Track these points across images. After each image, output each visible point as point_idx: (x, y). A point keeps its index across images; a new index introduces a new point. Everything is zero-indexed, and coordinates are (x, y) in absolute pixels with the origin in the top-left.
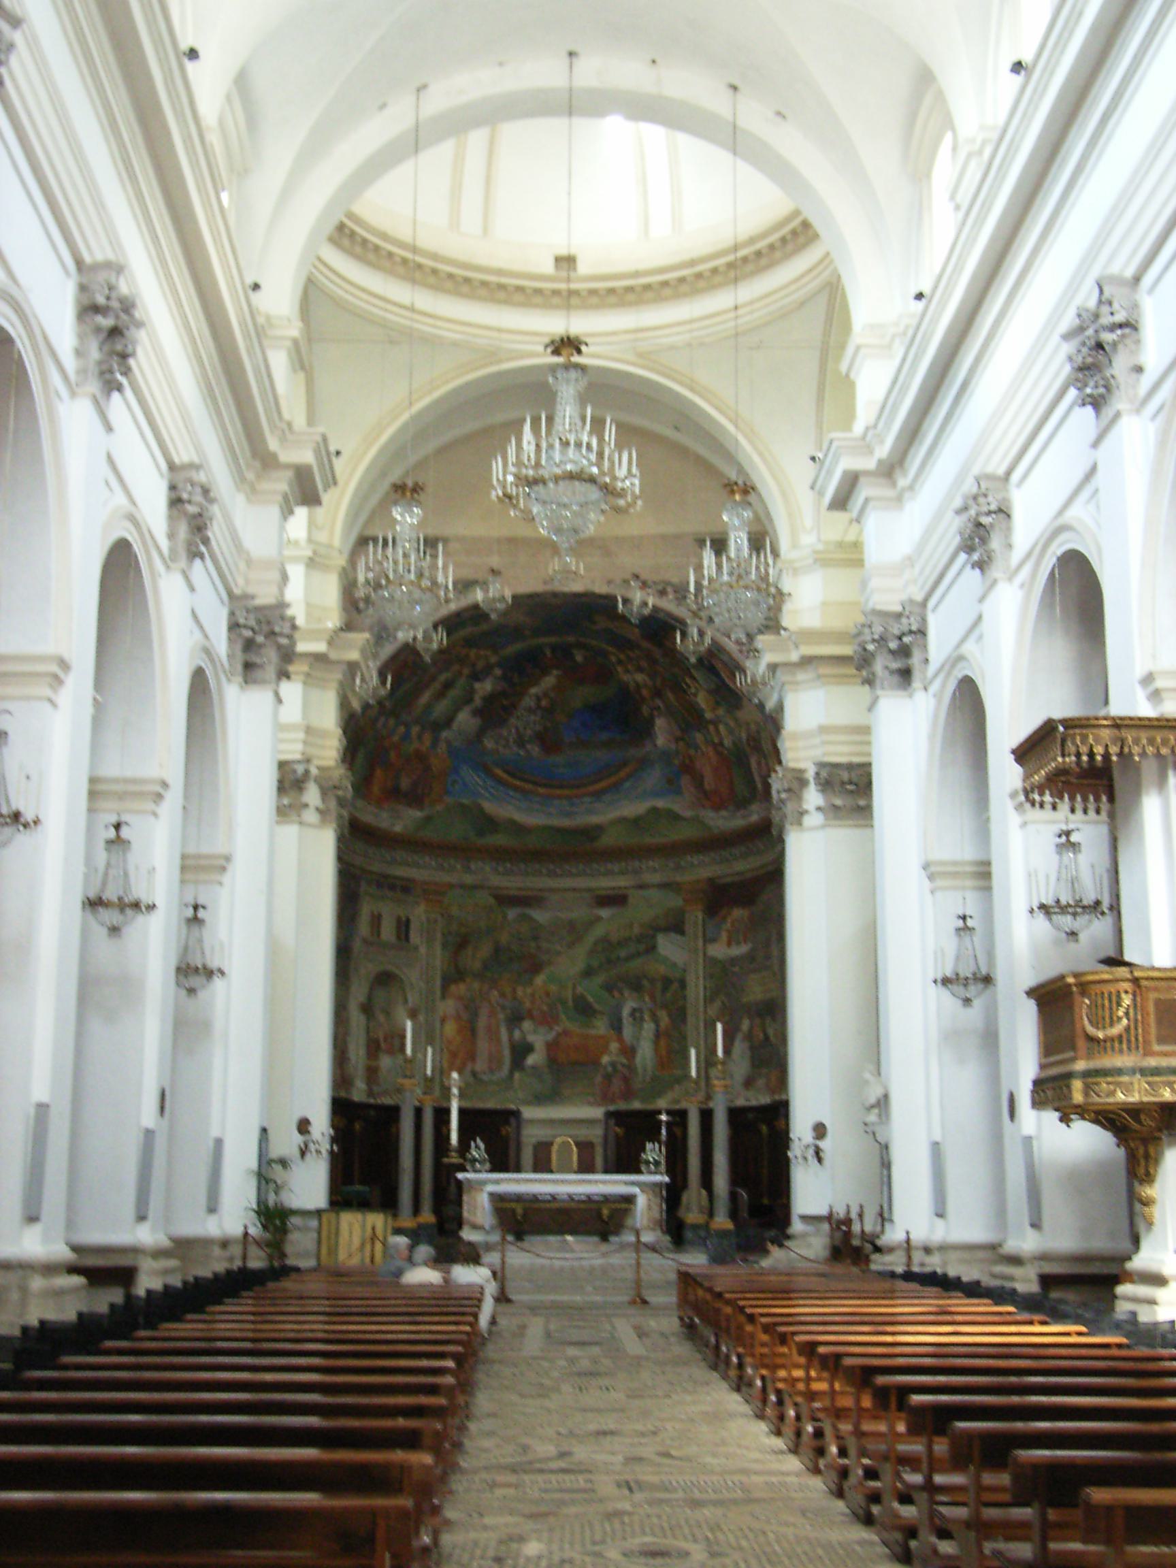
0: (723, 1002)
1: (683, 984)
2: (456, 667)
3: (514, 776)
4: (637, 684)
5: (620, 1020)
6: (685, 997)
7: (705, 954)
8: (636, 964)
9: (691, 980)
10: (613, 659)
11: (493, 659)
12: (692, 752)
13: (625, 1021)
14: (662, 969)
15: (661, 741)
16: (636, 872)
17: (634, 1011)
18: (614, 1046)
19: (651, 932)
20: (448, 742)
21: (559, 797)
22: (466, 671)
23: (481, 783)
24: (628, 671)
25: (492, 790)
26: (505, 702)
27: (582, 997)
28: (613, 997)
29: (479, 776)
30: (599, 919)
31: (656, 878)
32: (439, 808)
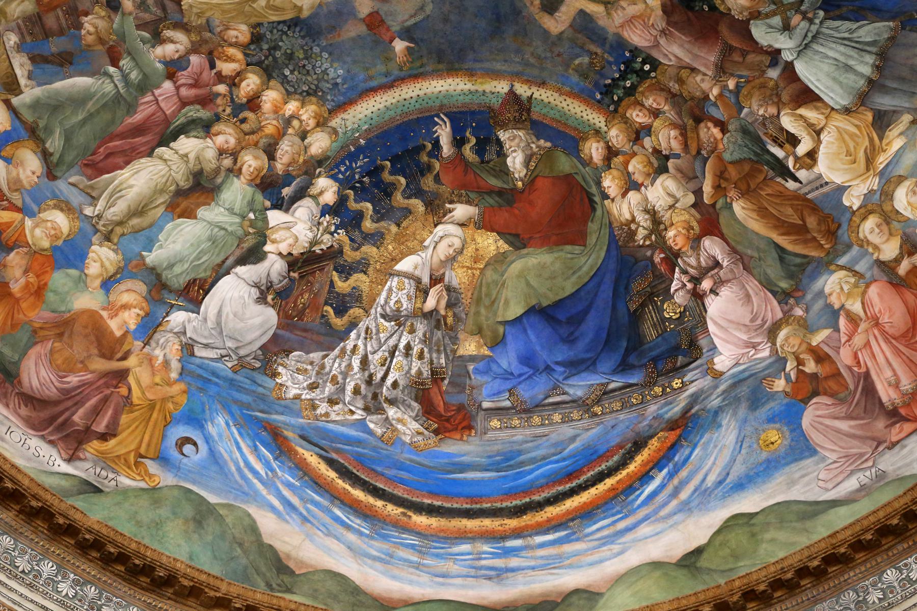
2: (226, 136)
3: (344, 473)
4: (652, 213)
10: (594, 150)
11: (319, 143)
12: (817, 339)
15: (722, 362)
20: (188, 349)
21: (463, 536)
22: (251, 162)
23: (258, 467)
24: (631, 185)
25: (286, 493)
26: (342, 286)
29: (255, 449)
32: (125, 481)
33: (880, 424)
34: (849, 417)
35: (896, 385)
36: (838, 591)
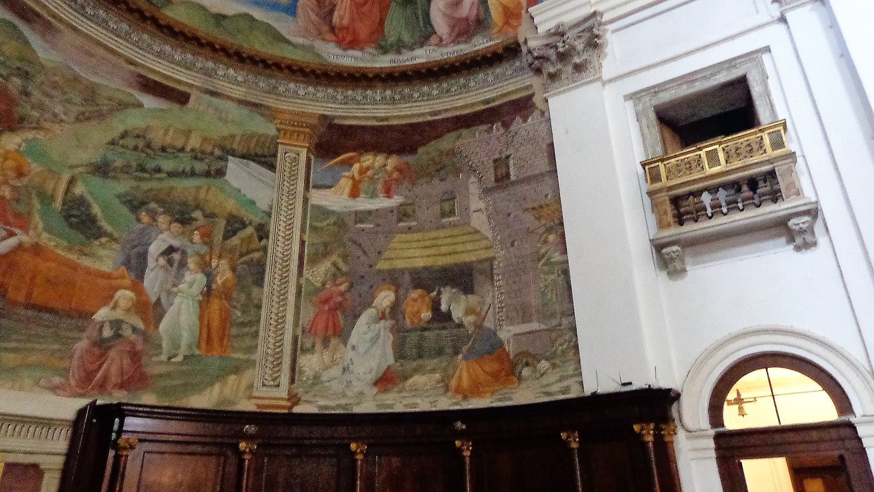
0: (334, 264)
1: (262, 232)
5: (143, 257)
6: (265, 249)
7: (306, 200)
8: (185, 187)
9: (278, 228)
13: (151, 263)
14: (230, 205)
16: (207, 73)
17: (171, 250)
18: (125, 296)
19: (217, 152)
27: (81, 202)
28: (139, 220)
30: (140, 105)
31: (238, 92)
33: (325, 28)
34: (317, 15)
35: (341, 19)
36: (270, 76)
